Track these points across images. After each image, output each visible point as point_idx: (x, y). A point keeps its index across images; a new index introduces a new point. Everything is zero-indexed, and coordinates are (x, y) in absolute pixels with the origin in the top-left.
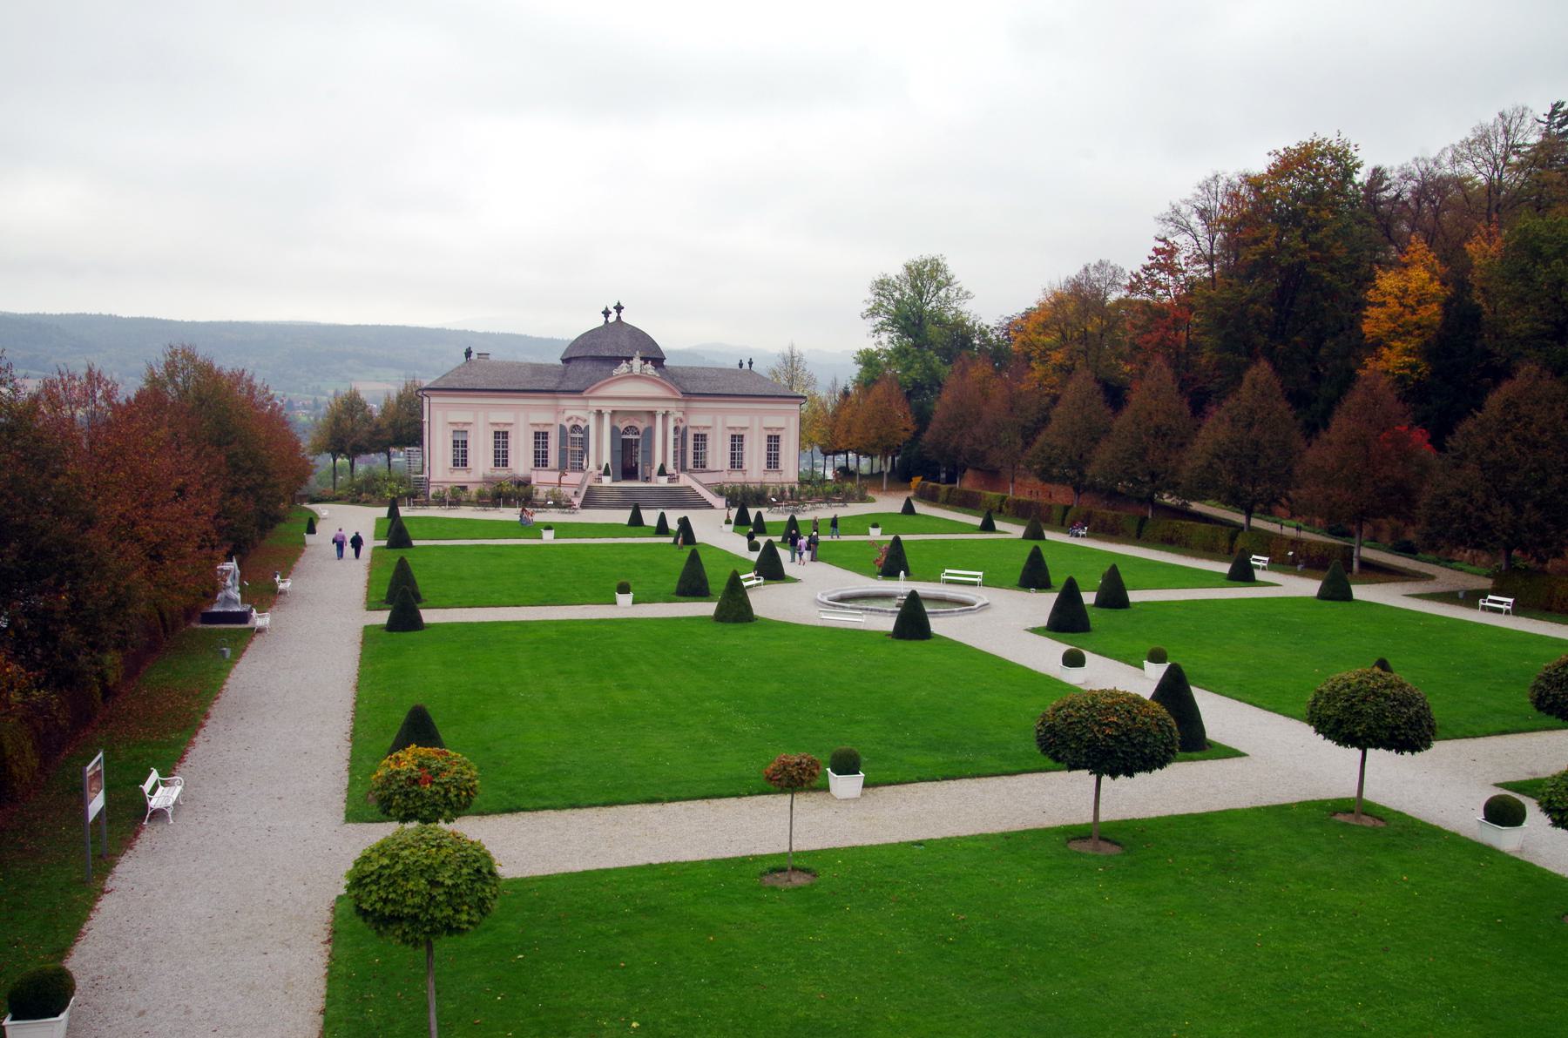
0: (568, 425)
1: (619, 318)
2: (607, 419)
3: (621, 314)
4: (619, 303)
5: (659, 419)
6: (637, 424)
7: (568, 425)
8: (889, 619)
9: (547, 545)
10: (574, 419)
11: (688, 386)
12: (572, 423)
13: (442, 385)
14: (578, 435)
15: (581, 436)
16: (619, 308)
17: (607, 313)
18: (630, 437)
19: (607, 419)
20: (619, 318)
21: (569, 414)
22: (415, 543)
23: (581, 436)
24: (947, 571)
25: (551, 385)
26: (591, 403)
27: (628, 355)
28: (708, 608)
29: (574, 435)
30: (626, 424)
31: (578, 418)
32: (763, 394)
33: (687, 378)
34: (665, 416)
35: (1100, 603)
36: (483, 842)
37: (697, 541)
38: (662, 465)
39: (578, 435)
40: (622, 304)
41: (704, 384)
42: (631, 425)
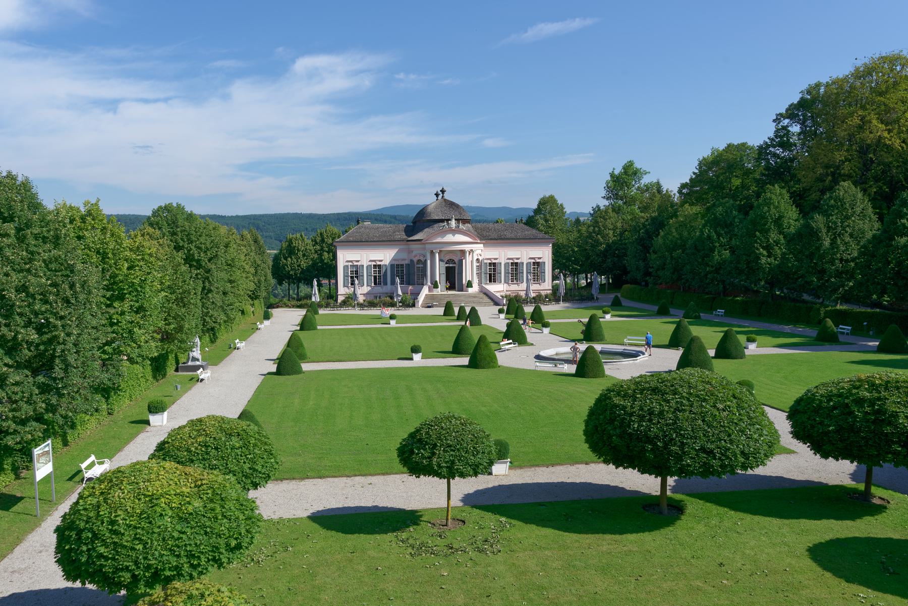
0: (415, 260)
1: (443, 197)
7: (415, 260)
8: (465, 358)
9: (393, 328)
14: (421, 266)
15: (422, 266)
16: (443, 191)
17: (437, 195)
18: (451, 265)
19: (437, 255)
22: (319, 327)
23: (422, 266)
26: (427, 246)
27: (448, 218)
28: (465, 361)
29: (418, 266)
30: (447, 258)
34: (471, 251)
35: (718, 356)
36: (258, 502)
37: (482, 323)
39: (421, 266)
40: (445, 189)
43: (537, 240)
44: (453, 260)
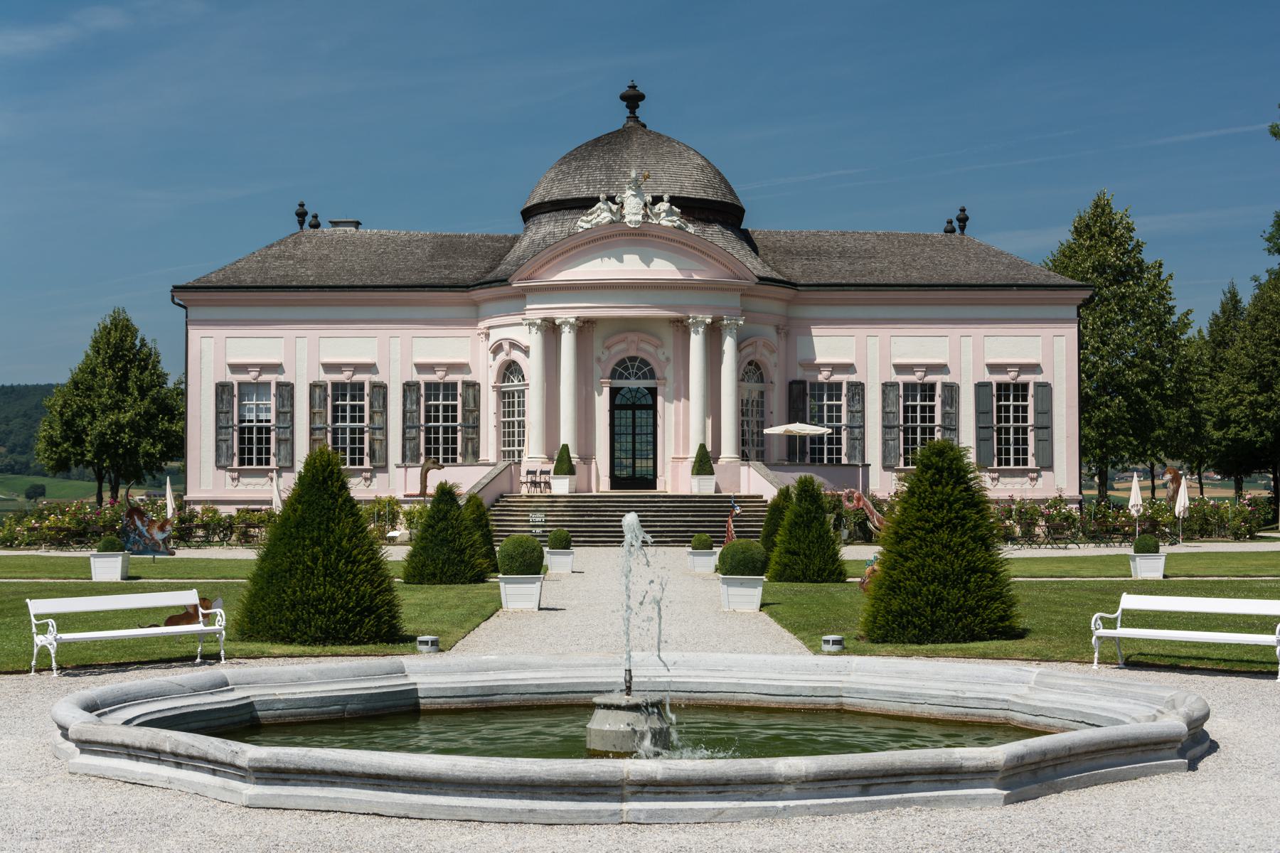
2: (567, 340)
3: (638, 112)
4: (634, 87)
5: (696, 342)
6: (646, 350)
10: (506, 346)
11: (795, 271)
12: (502, 357)
13: (214, 280)
18: (633, 383)
19: (567, 340)
20: (633, 117)
21: (496, 335)
24: (1130, 602)
25: (468, 275)
30: (621, 350)
31: (514, 345)
32: (982, 281)
33: (798, 253)
38: (703, 447)
40: (641, 89)
41: (838, 264)
42: (633, 353)
43: (1014, 294)
44: (645, 363)
